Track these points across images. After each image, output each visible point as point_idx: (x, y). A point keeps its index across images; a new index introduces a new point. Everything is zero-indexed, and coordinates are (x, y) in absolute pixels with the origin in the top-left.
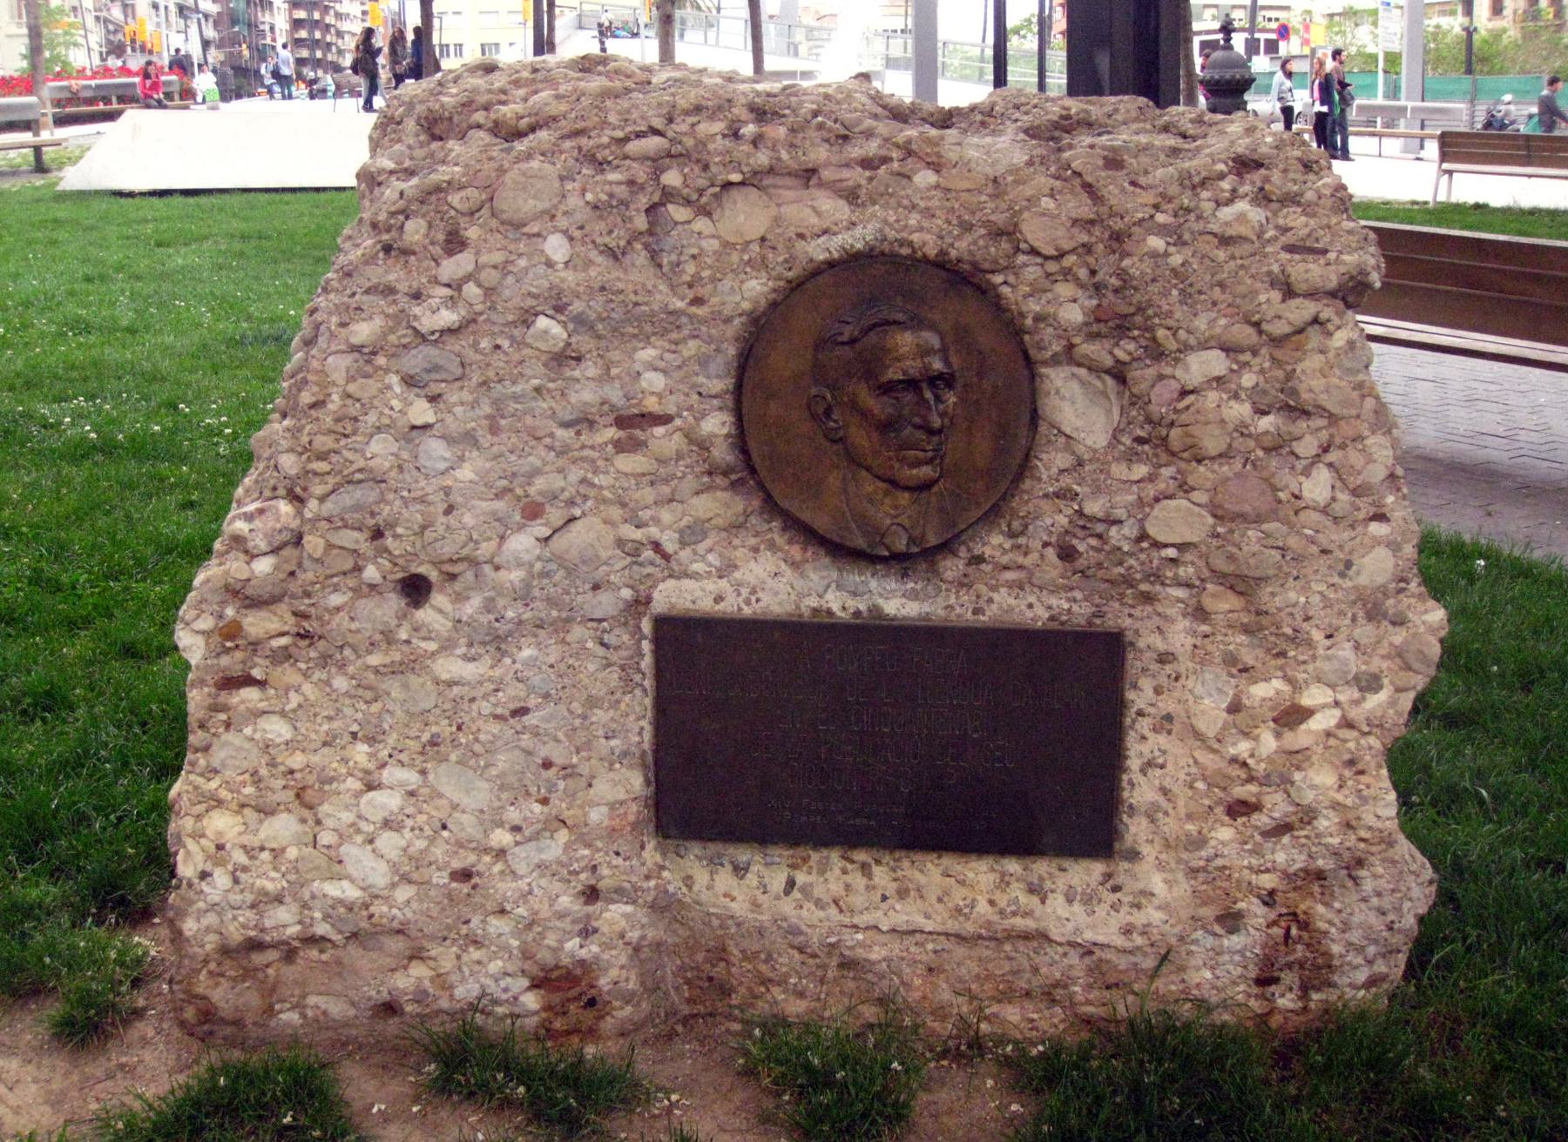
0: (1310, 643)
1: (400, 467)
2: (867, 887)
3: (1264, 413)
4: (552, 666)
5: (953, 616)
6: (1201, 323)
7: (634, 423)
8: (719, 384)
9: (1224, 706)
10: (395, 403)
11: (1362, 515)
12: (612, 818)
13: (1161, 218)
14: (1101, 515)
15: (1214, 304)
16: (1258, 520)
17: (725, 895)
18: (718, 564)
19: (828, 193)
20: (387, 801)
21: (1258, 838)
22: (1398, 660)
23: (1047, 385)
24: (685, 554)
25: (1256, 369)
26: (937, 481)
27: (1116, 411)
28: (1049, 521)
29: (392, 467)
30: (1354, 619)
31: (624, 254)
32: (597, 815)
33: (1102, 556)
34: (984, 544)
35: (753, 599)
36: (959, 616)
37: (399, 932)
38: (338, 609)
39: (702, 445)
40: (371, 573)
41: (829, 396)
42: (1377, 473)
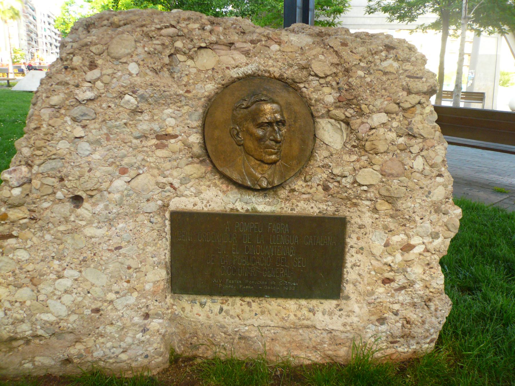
0: (415, 221)
1: (70, 153)
2: (250, 310)
3: (401, 137)
4: (131, 230)
5: (283, 212)
6: (378, 103)
7: (163, 137)
9: (383, 244)
10: (69, 128)
11: (434, 175)
12: (153, 287)
13: (362, 64)
14: (339, 174)
15: (382, 96)
16: (398, 176)
17: (197, 314)
18: (194, 191)
19: (238, 52)
20: (66, 283)
21: (393, 291)
22: (445, 227)
23: (319, 126)
24: (182, 188)
25: (398, 120)
26: (278, 161)
27: (345, 135)
28: (320, 176)
29: (67, 154)
30: (430, 213)
31: (160, 72)
32: (148, 287)
33: (339, 189)
34: (295, 185)
35: (208, 205)
36: (286, 211)
37: (71, 332)
38: (46, 209)
39: (190, 147)
40: (59, 195)
41: (238, 128)
42: (439, 159)
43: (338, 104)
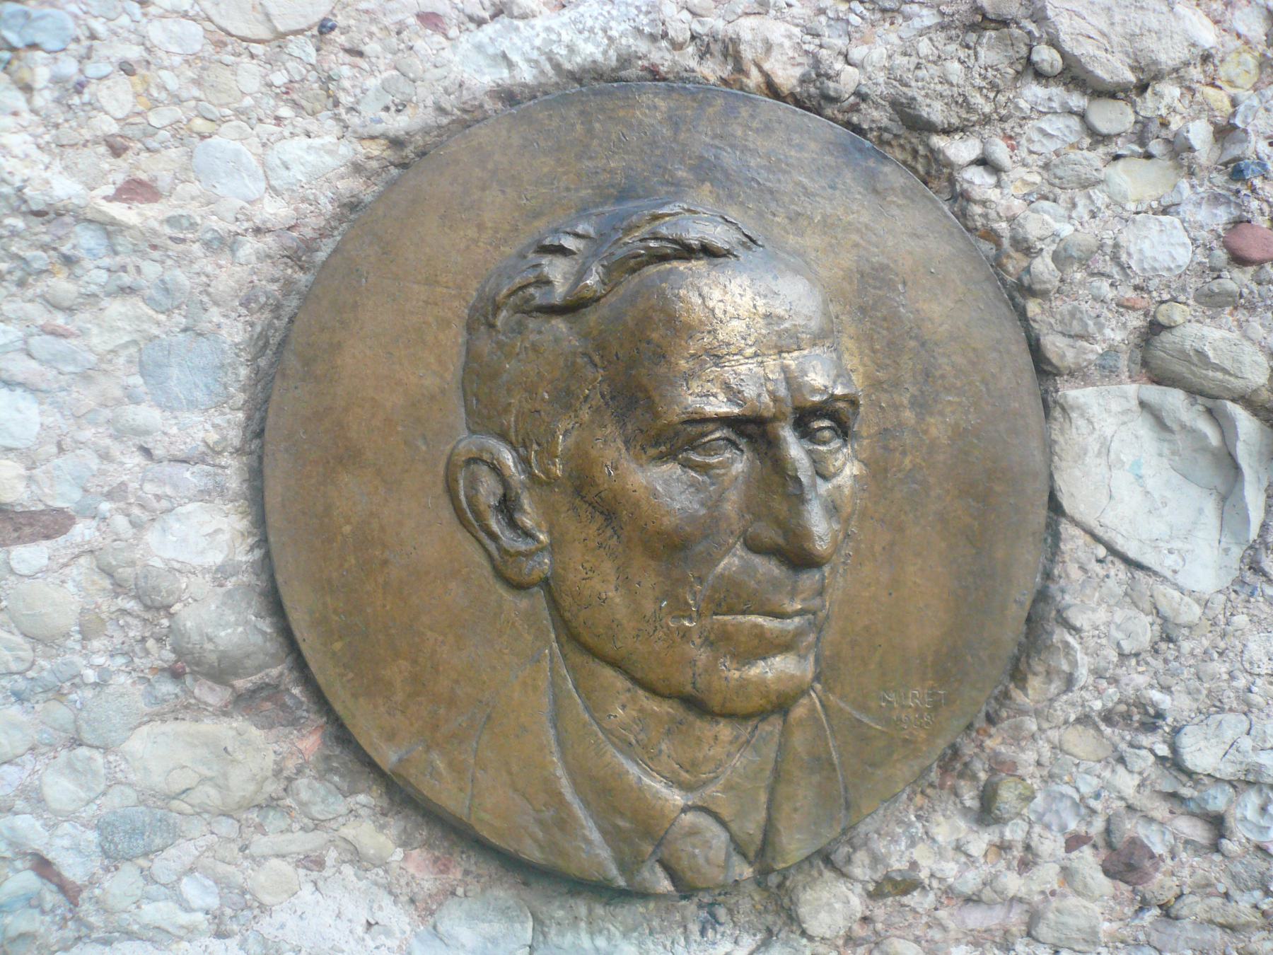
8: (213, 424)
14: (1228, 770)
18: (213, 902)
24: (121, 885)
26: (804, 692)
27: (1254, 499)
28: (1088, 785)
34: (913, 843)
39: (154, 603)
41: (508, 458)
43: (1236, 280)
